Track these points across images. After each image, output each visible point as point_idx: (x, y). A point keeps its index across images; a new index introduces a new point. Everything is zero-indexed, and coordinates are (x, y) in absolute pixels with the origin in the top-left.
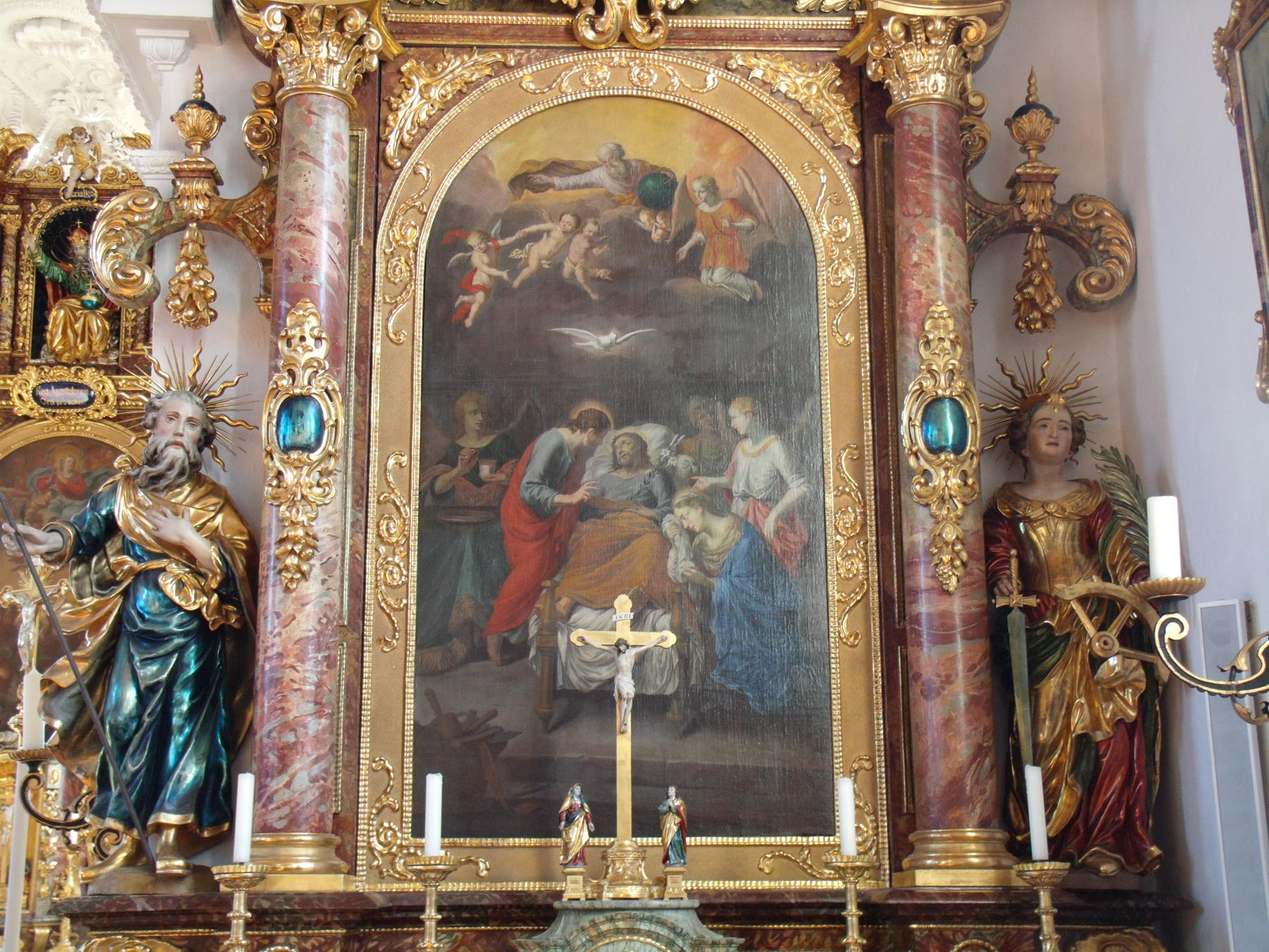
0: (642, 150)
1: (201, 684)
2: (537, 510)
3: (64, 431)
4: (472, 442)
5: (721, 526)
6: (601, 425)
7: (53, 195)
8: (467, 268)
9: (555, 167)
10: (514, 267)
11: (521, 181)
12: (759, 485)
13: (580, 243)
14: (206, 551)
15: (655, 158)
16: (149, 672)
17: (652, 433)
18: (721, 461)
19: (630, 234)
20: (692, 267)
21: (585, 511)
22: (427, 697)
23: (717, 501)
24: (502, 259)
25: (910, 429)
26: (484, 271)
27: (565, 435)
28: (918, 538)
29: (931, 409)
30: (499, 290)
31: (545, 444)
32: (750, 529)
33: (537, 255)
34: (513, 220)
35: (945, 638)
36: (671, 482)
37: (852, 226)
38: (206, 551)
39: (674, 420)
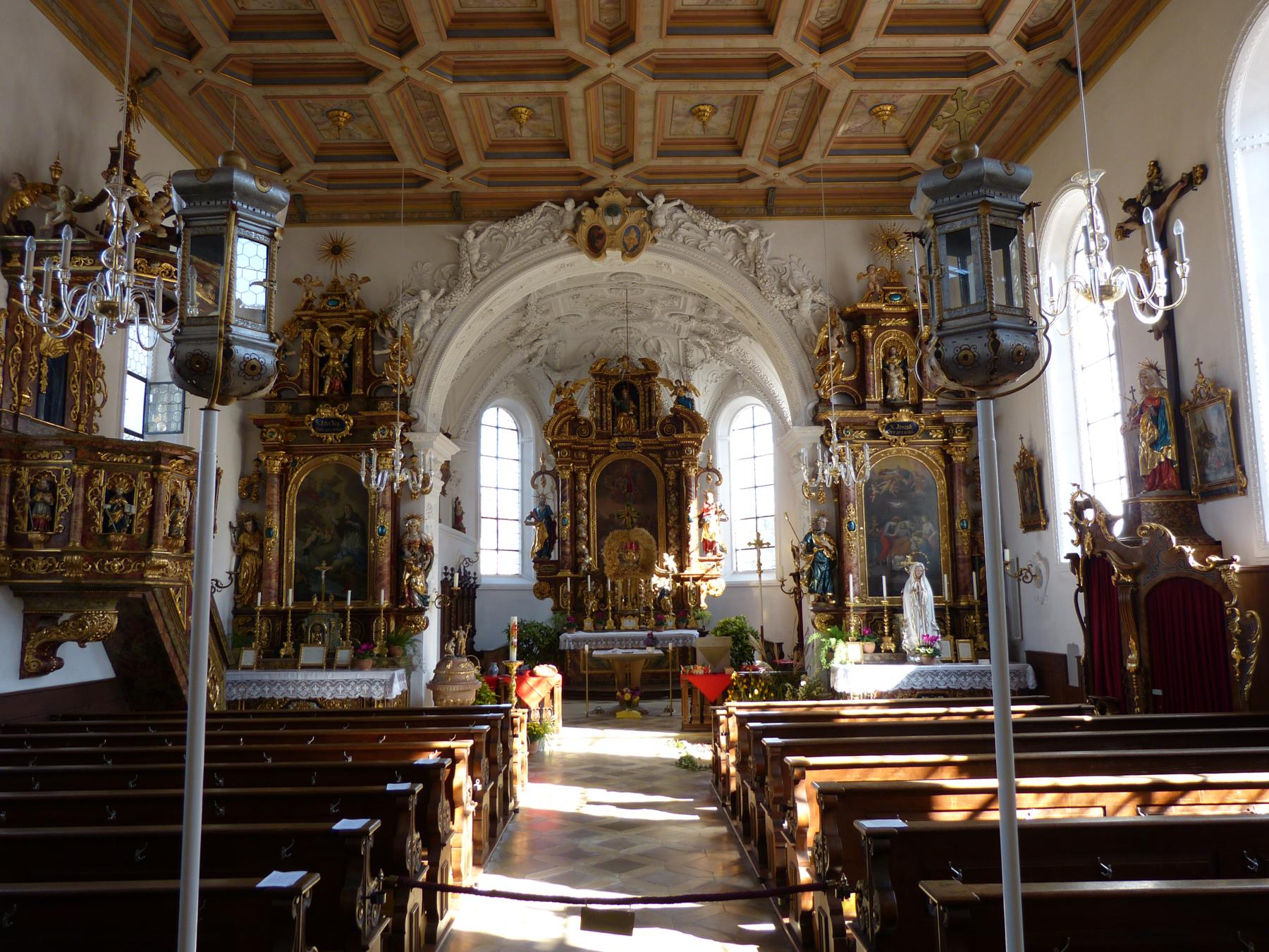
0: (903, 466)
1: (830, 571)
2: (886, 537)
3: (625, 457)
4: (874, 525)
5: (921, 540)
6: (898, 521)
7: (617, 377)
8: (871, 491)
9: (887, 470)
10: (880, 490)
11: (881, 473)
12: (927, 532)
13: (892, 486)
14: (831, 547)
15: (906, 468)
16: (823, 569)
17: (907, 522)
18: (920, 528)
19: (902, 484)
20: (913, 490)
21: (897, 537)
22: (869, 572)
23: (920, 535)
24: (878, 489)
25: (958, 524)
26: (875, 491)
27: (893, 523)
28: (959, 544)
29: (962, 521)
30: (877, 495)
31: (888, 525)
32: (926, 540)
33: (884, 488)
34: (880, 481)
35: (964, 562)
36: (911, 531)
37: (944, 482)
38: (831, 547)
39: (912, 520)
